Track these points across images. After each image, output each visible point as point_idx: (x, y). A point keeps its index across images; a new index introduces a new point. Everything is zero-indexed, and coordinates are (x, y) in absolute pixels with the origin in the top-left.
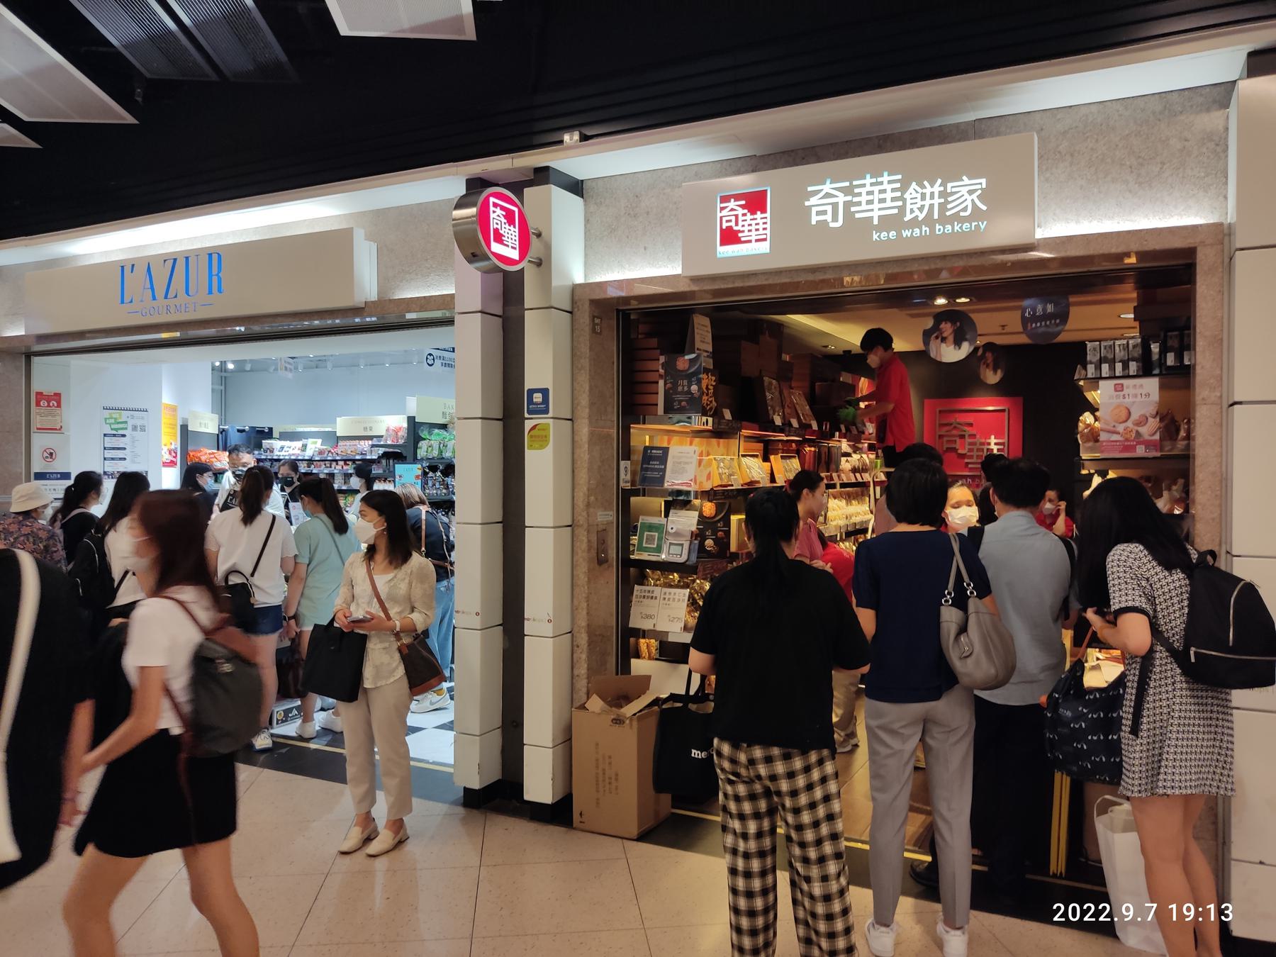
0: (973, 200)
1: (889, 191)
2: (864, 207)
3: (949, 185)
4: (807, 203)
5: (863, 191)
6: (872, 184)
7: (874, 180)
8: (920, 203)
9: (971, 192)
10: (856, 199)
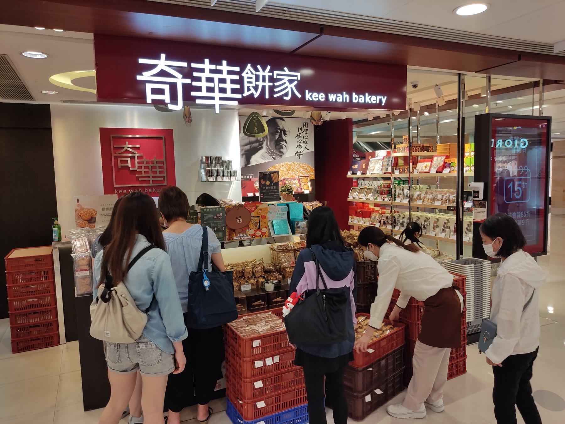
0: (291, 88)
9: (291, 81)
10: (195, 84)
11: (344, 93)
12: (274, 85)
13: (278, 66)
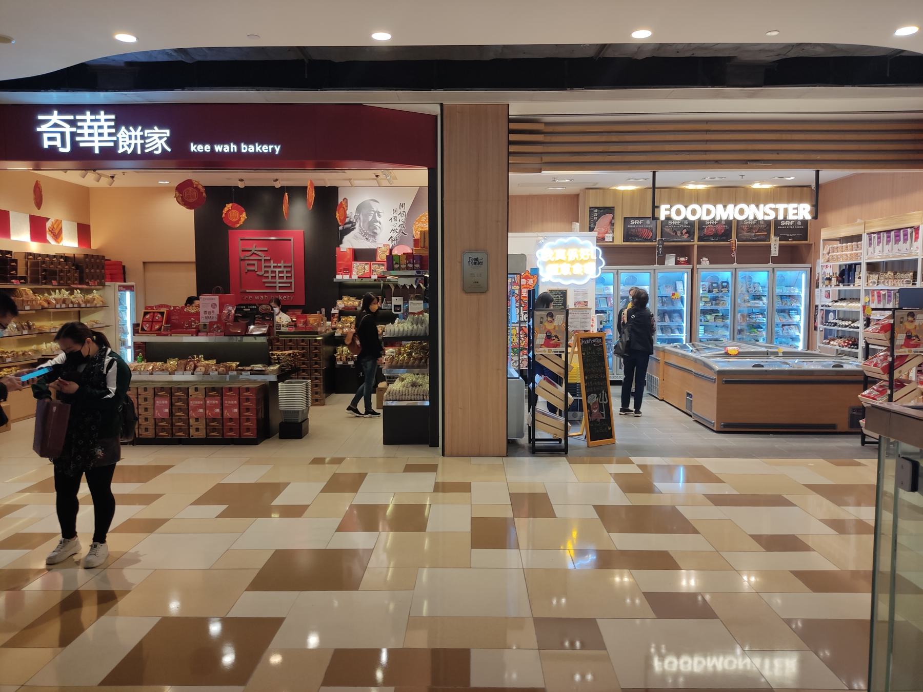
1: (106, 127)
2: (86, 138)
3: (146, 131)
4: (38, 130)
5: (85, 125)
6: (92, 120)
7: (93, 117)
8: (128, 142)
9: (160, 138)
11: (232, 144)
12: (145, 142)
13: (147, 125)
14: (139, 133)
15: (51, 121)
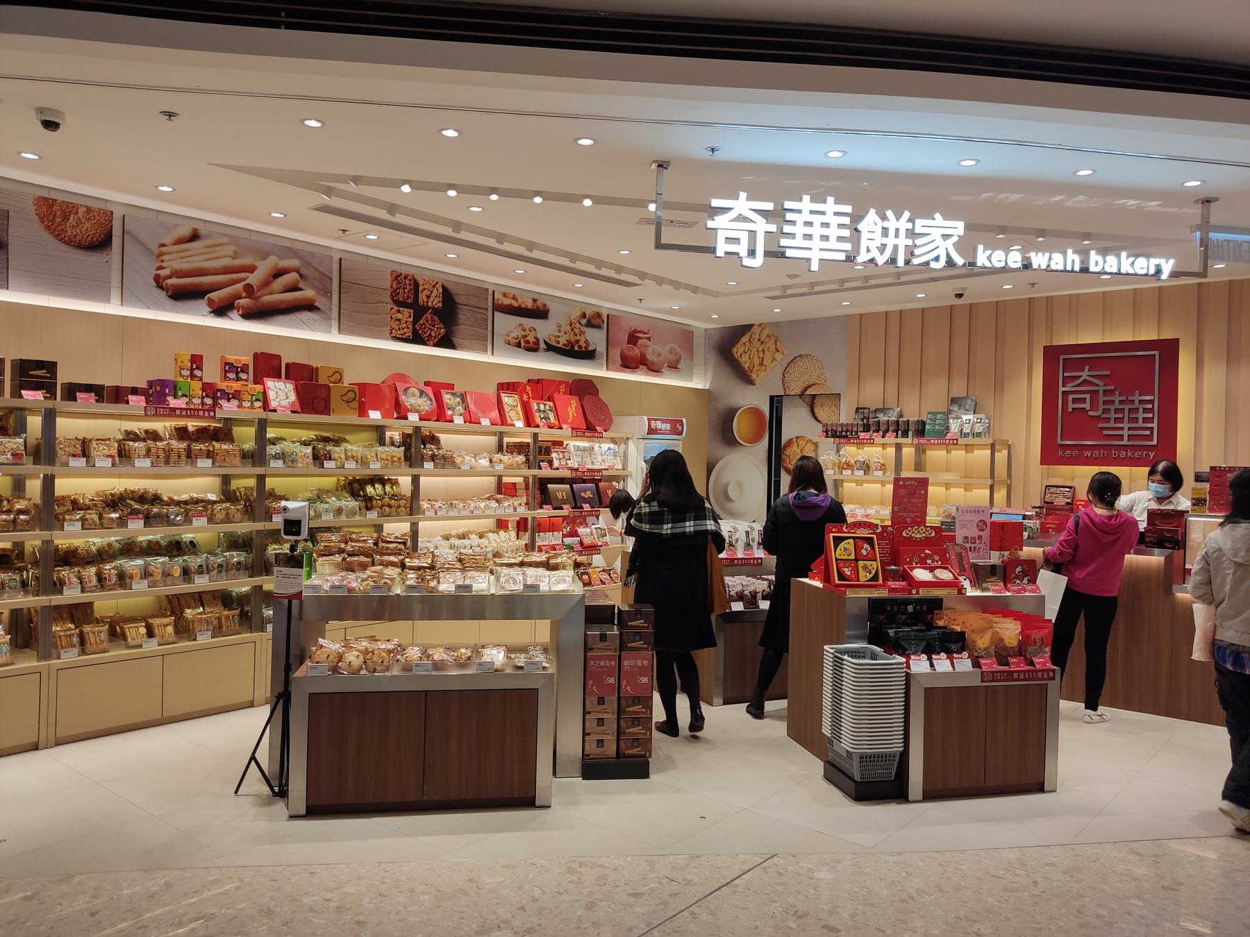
2: (799, 241)
4: (710, 224)
6: (812, 212)
11: (1070, 251)
14: (904, 224)
15: (732, 212)
